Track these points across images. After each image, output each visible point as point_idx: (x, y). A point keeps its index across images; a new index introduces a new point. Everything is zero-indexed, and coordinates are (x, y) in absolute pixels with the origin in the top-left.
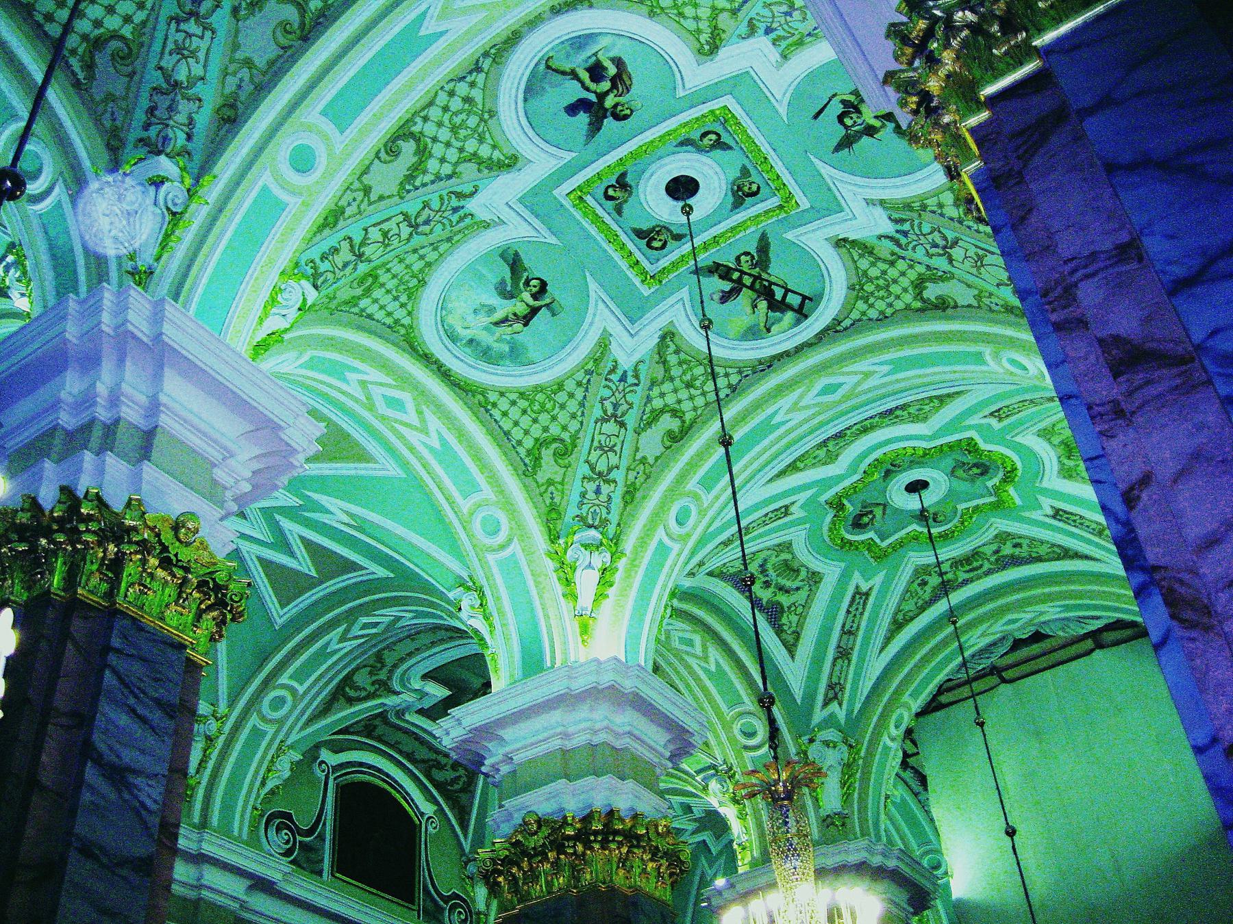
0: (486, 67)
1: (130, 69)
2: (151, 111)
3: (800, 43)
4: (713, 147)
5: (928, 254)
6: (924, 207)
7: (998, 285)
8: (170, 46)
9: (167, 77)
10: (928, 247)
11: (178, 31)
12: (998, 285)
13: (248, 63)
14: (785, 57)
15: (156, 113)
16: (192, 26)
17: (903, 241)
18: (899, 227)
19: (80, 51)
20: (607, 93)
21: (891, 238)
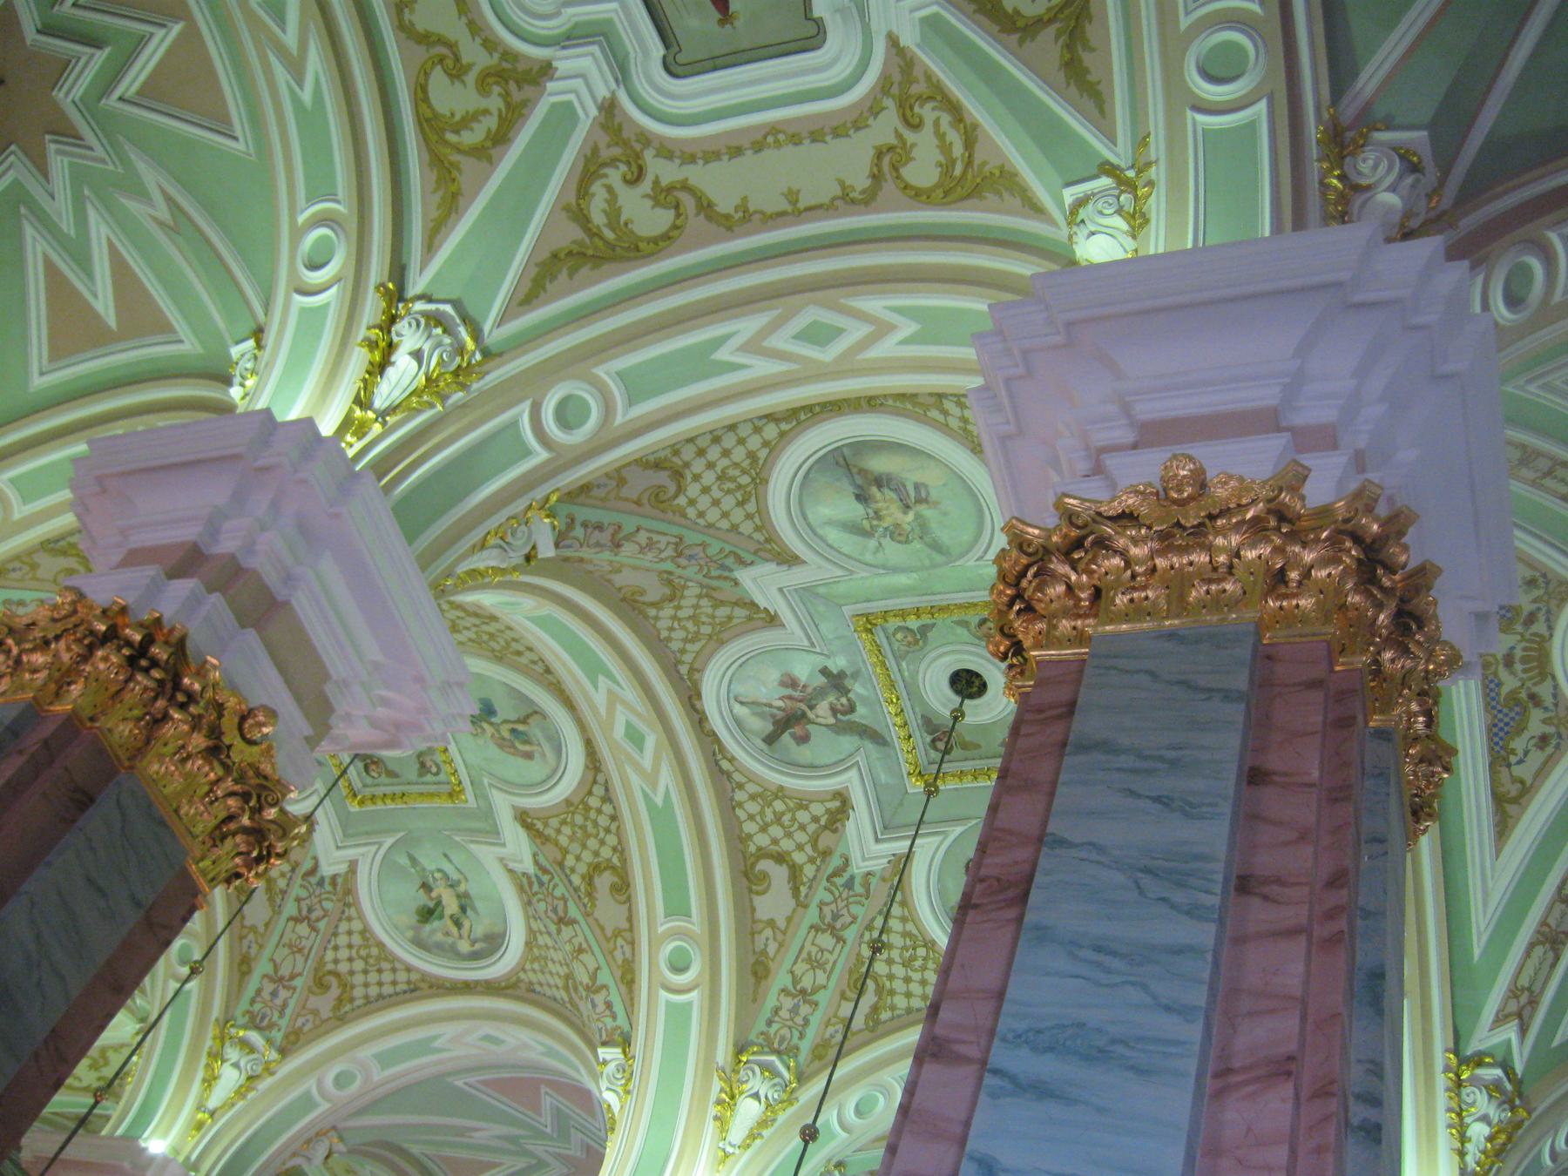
0: (549, 677)
1: (645, 501)
2: (599, 527)
3: (521, 889)
4: (423, 765)
5: (298, 900)
6: (349, 905)
7: (272, 960)
8: (656, 537)
9: (628, 538)
10: (308, 902)
11: (668, 543)
12: (272, 960)
13: (618, 571)
14: (511, 871)
15: (597, 532)
16: (669, 552)
17: (314, 880)
18: (327, 881)
19: (675, 459)
20: (498, 731)
21: (314, 870)
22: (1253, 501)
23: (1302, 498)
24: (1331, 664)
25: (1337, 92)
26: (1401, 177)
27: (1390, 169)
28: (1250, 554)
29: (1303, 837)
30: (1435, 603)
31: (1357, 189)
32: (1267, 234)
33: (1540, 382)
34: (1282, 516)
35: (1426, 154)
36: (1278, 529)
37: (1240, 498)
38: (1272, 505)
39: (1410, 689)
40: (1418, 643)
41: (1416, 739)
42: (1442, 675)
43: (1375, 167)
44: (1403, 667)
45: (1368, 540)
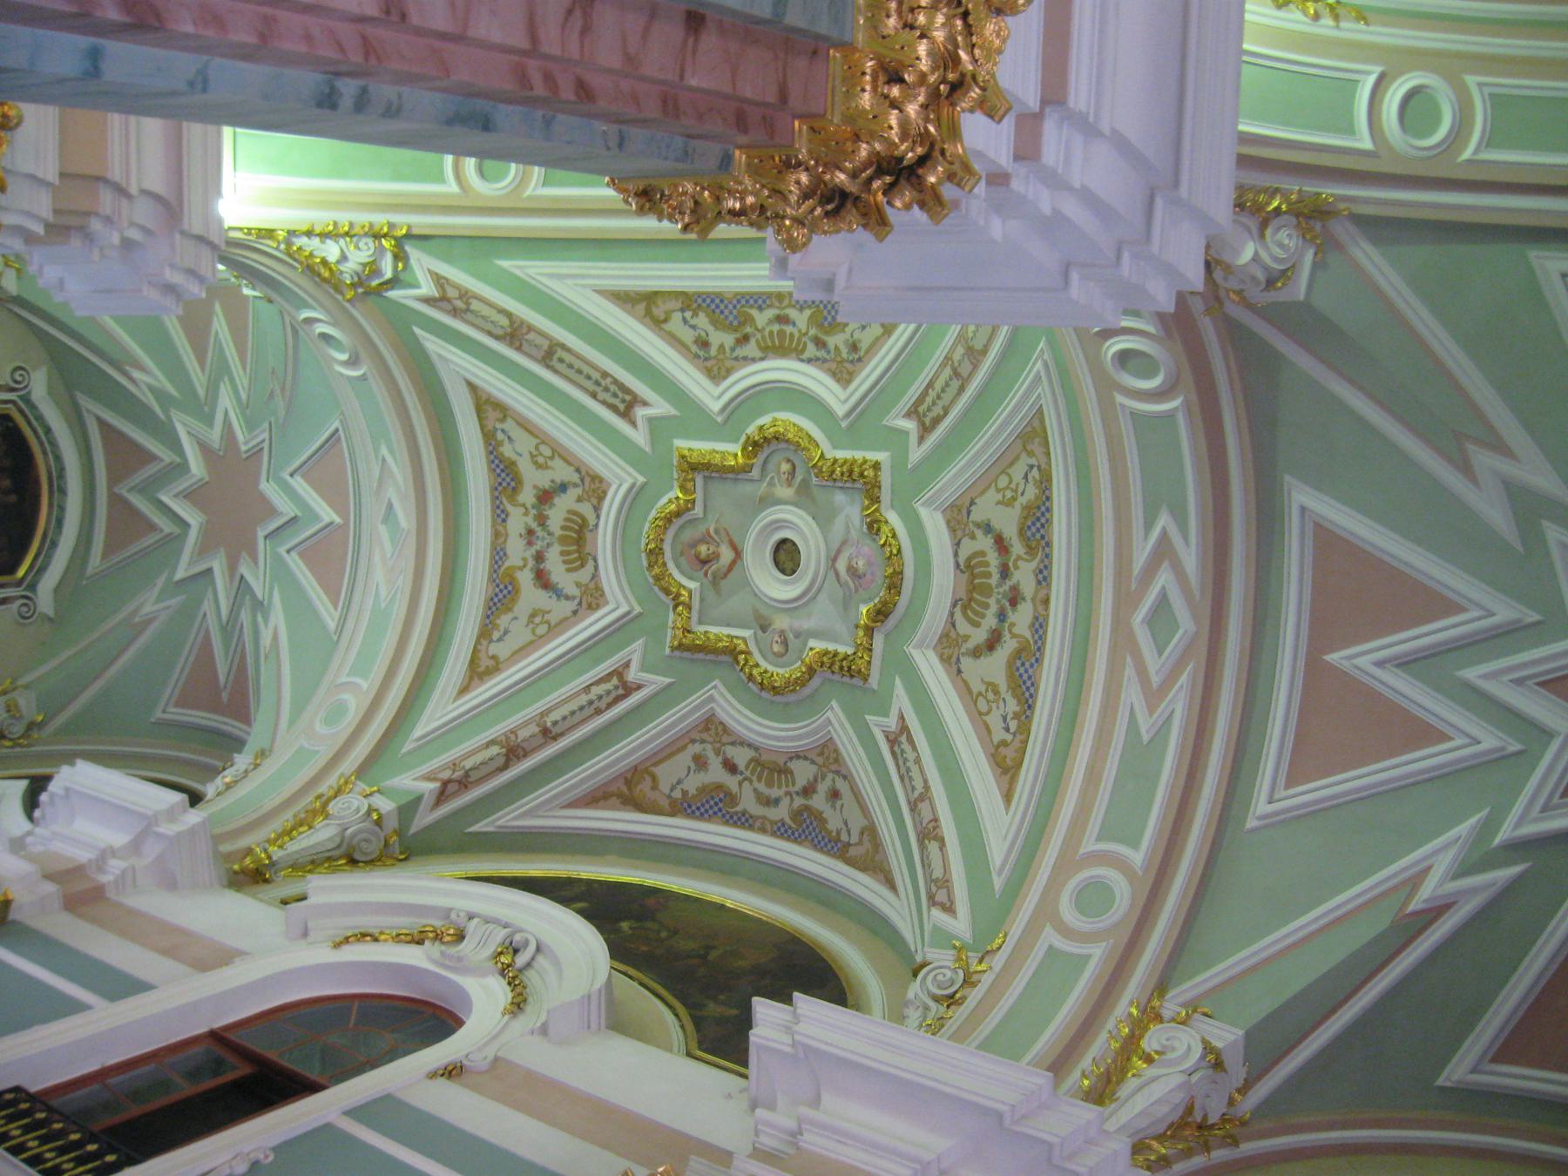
22: (976, 61)
23: (972, 111)
24: (800, 117)
25: (1361, 221)
26: (1266, 268)
27: (1276, 259)
28: (922, 48)
29: (629, 59)
30: (851, 230)
31: (1264, 224)
32: (1242, 128)
33: (1042, 374)
34: (957, 87)
35: (1280, 296)
36: (944, 81)
37: (981, 48)
38: (969, 78)
39: (769, 197)
40: (812, 210)
41: (718, 199)
42: (778, 232)
43: (1281, 245)
44: (790, 192)
45: (920, 171)
